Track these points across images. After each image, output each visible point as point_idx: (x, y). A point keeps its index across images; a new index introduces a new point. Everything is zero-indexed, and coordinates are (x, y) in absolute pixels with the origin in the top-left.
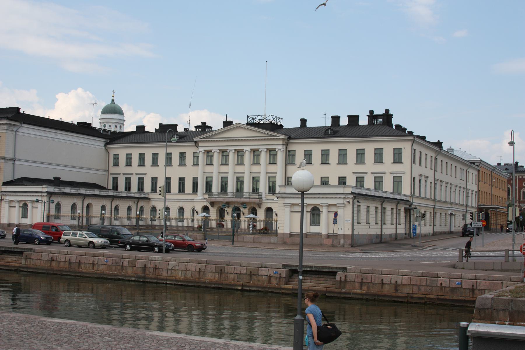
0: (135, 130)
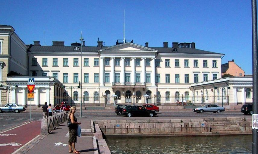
0: (33, 44)
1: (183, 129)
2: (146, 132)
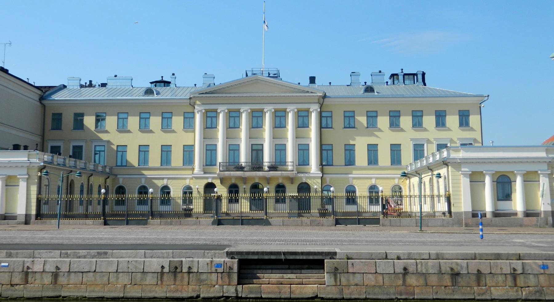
1: (165, 277)
2: (71, 282)
